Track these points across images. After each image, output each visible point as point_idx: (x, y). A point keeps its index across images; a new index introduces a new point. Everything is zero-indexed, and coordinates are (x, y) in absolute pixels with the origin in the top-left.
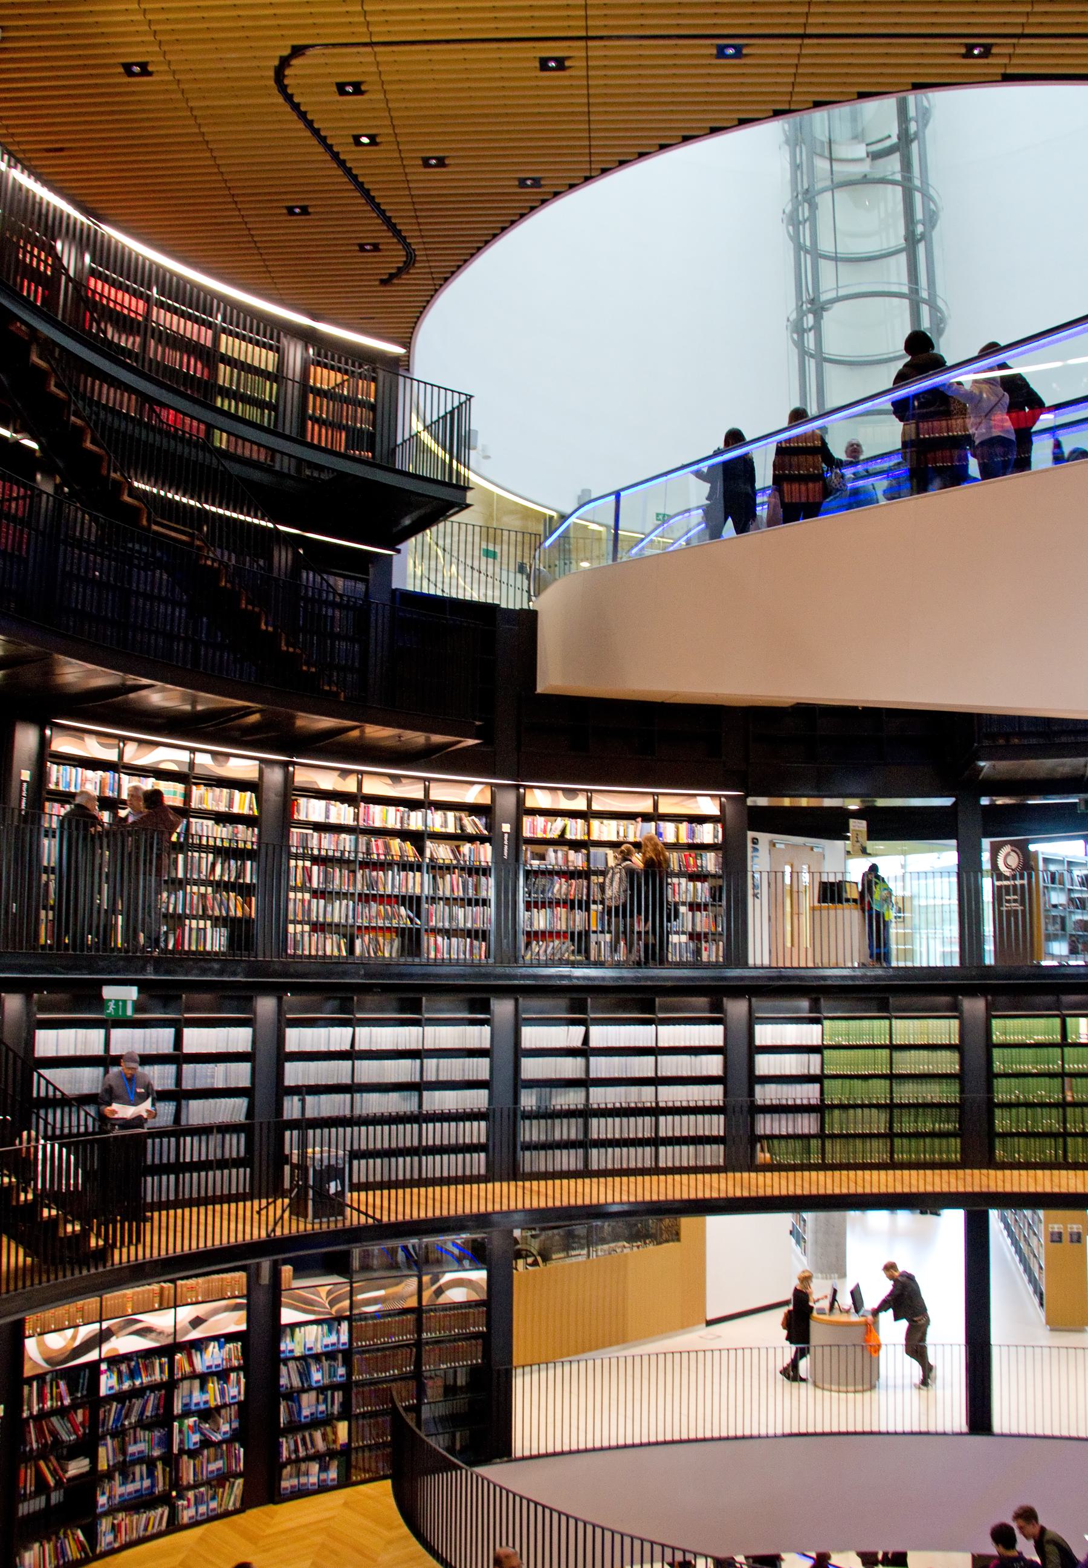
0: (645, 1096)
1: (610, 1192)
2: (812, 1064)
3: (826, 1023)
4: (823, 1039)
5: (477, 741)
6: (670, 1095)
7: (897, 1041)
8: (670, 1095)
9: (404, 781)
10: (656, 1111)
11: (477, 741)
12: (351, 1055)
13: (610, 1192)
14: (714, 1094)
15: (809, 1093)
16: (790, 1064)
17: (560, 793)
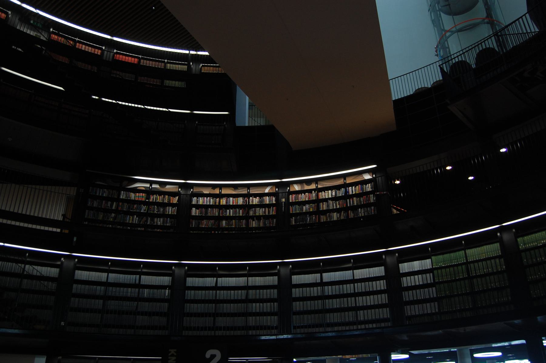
0: (351, 302)
1: (37, 211)
2: (429, 278)
3: (433, 258)
4: (432, 266)
5: (64, 90)
6: (361, 301)
7: (470, 260)
8: (361, 301)
9: (239, 188)
10: (357, 309)
11: (64, 90)
12: (216, 288)
13: (37, 211)
14: (383, 298)
15: (432, 292)
16: (418, 280)
17: (304, 184)
